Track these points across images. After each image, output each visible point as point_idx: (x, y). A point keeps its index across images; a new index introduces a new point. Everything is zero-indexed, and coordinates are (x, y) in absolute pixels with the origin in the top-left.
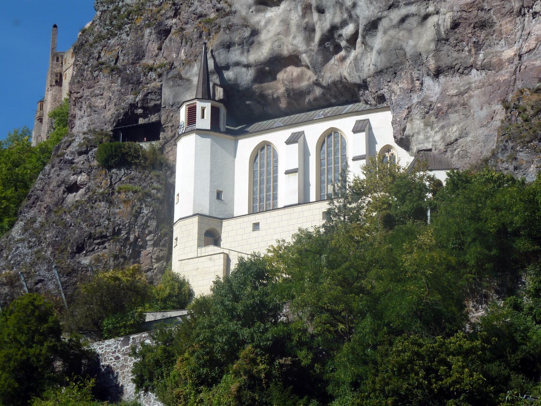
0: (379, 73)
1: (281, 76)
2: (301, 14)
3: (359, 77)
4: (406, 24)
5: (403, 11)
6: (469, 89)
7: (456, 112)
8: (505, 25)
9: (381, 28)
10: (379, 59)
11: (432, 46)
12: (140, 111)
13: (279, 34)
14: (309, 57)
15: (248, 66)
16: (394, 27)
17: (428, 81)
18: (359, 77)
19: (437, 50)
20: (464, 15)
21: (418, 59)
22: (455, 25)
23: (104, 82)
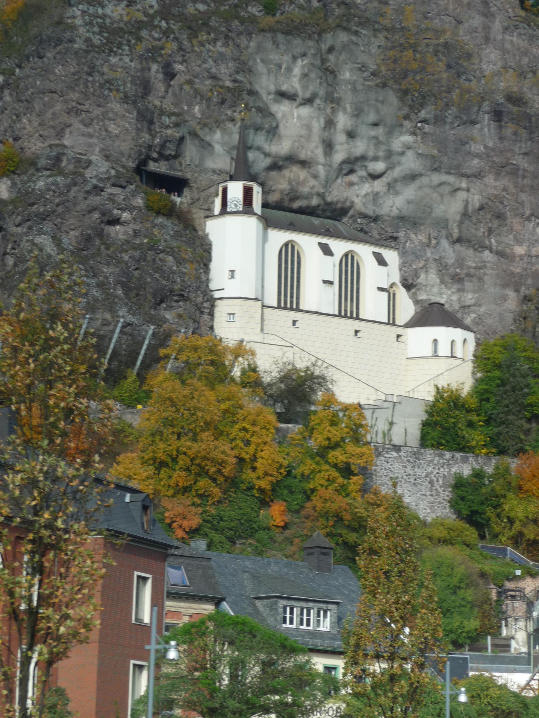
0: (401, 218)
1: (286, 173)
2: (323, 126)
3: (374, 211)
4: (441, 189)
5: (444, 178)
6: (485, 267)
7: (471, 281)
8: (515, 223)
9: (418, 182)
10: (406, 207)
11: (458, 218)
12: (155, 155)
13: (301, 136)
14: (326, 171)
15: (266, 155)
16: (431, 187)
17: (445, 243)
18: (374, 211)
19: (461, 223)
20: (490, 203)
21: (442, 223)
22: (481, 208)
23: (116, 106)
